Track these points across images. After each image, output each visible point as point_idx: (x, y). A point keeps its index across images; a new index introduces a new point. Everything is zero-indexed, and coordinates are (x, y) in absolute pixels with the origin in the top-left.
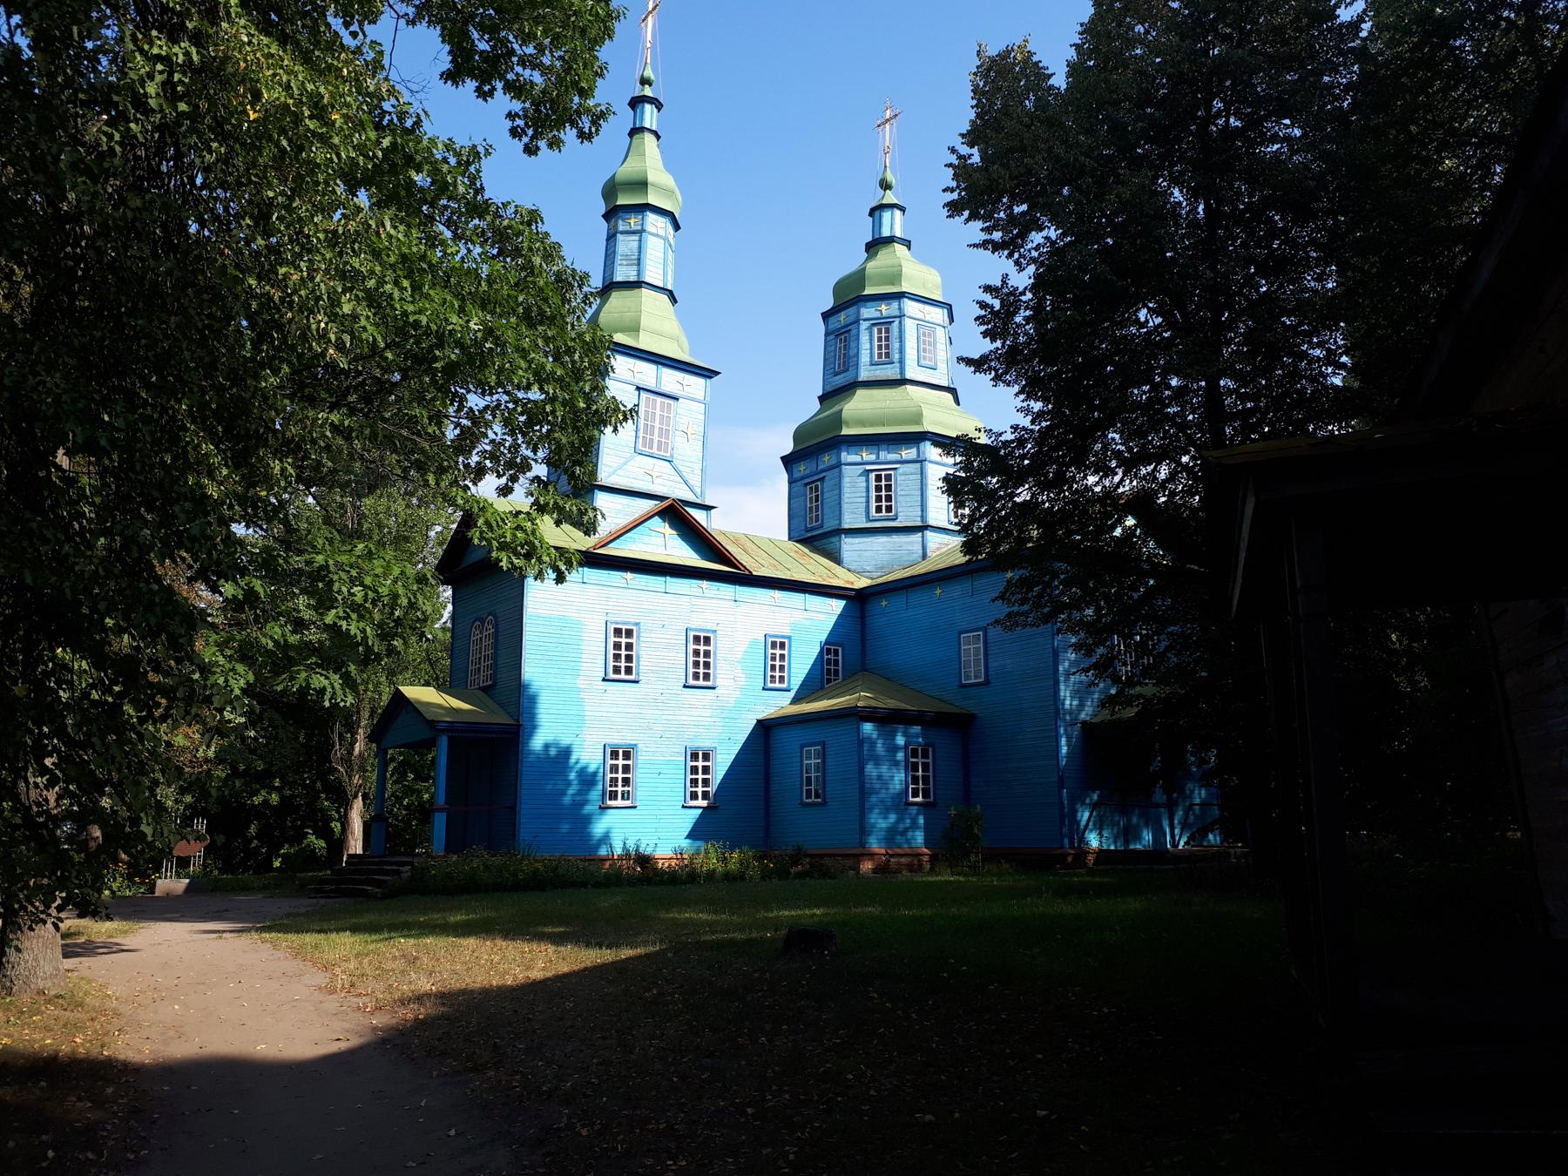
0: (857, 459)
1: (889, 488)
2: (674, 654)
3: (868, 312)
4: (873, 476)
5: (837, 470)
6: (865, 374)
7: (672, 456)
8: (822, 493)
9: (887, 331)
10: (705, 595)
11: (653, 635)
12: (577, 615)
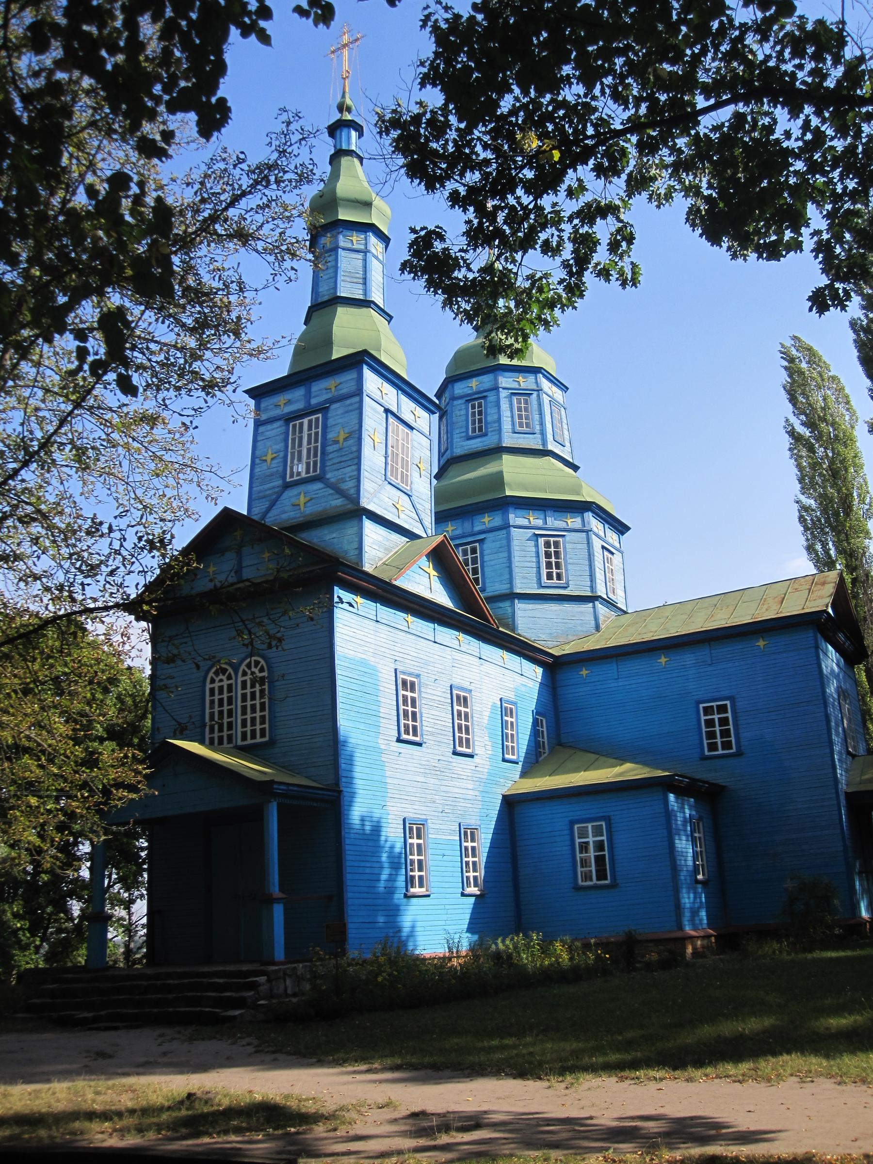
0: (525, 522)
1: (557, 554)
2: (443, 715)
3: (505, 381)
4: (542, 541)
6: (507, 442)
7: (411, 490)
9: (526, 402)
10: (462, 649)
11: (429, 691)
12: (373, 659)
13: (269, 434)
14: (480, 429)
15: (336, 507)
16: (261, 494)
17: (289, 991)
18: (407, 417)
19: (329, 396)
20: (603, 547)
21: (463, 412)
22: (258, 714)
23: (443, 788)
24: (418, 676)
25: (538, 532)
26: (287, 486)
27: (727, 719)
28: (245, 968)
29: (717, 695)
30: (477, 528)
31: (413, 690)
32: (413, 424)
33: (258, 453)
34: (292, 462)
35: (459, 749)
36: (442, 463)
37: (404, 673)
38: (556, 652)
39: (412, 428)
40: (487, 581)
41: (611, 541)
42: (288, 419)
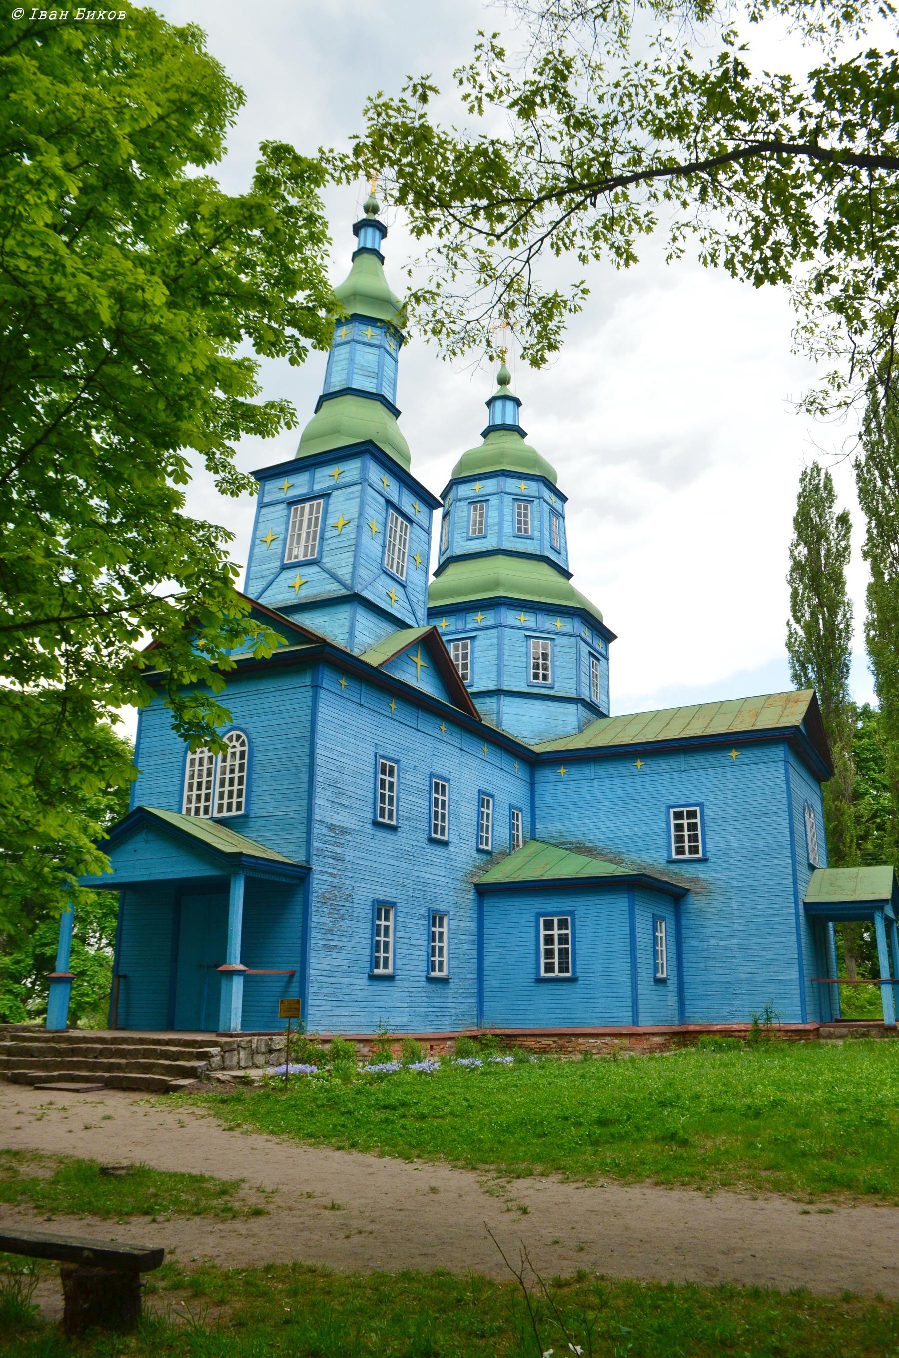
0: (517, 623)
5: (495, 630)
8: (473, 652)
9: (526, 508)
11: (407, 777)
13: (271, 516)
14: (481, 530)
15: (330, 591)
16: (259, 575)
17: (242, 1064)
18: (407, 509)
19: (332, 483)
20: (590, 652)
21: (465, 514)
22: (236, 788)
23: (414, 873)
24: (397, 762)
25: (528, 633)
26: (284, 567)
27: (695, 824)
28: (199, 1037)
29: (688, 801)
30: (469, 626)
31: (391, 774)
32: (413, 518)
33: (259, 533)
34: (292, 544)
35: (433, 836)
36: (442, 560)
37: (383, 757)
38: (538, 749)
39: (410, 521)
40: (476, 677)
41: (597, 647)
42: (291, 503)
